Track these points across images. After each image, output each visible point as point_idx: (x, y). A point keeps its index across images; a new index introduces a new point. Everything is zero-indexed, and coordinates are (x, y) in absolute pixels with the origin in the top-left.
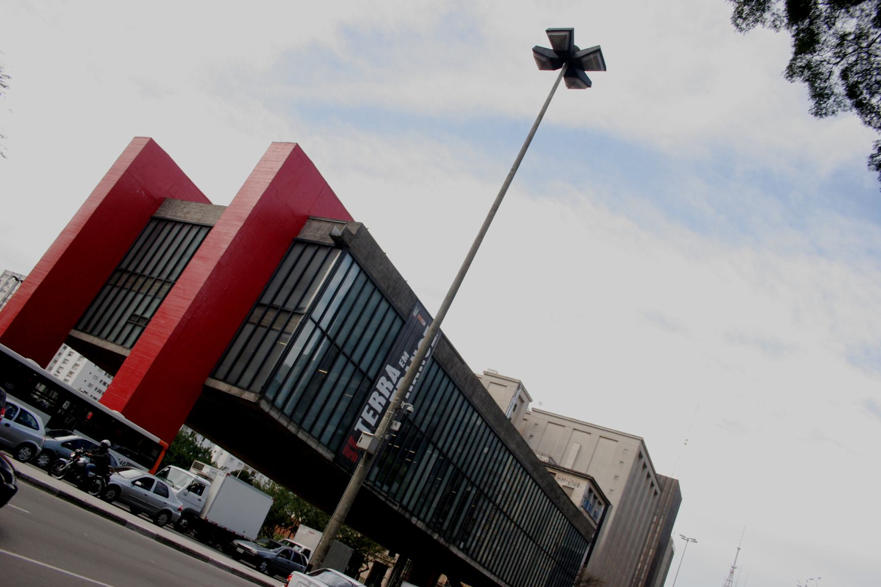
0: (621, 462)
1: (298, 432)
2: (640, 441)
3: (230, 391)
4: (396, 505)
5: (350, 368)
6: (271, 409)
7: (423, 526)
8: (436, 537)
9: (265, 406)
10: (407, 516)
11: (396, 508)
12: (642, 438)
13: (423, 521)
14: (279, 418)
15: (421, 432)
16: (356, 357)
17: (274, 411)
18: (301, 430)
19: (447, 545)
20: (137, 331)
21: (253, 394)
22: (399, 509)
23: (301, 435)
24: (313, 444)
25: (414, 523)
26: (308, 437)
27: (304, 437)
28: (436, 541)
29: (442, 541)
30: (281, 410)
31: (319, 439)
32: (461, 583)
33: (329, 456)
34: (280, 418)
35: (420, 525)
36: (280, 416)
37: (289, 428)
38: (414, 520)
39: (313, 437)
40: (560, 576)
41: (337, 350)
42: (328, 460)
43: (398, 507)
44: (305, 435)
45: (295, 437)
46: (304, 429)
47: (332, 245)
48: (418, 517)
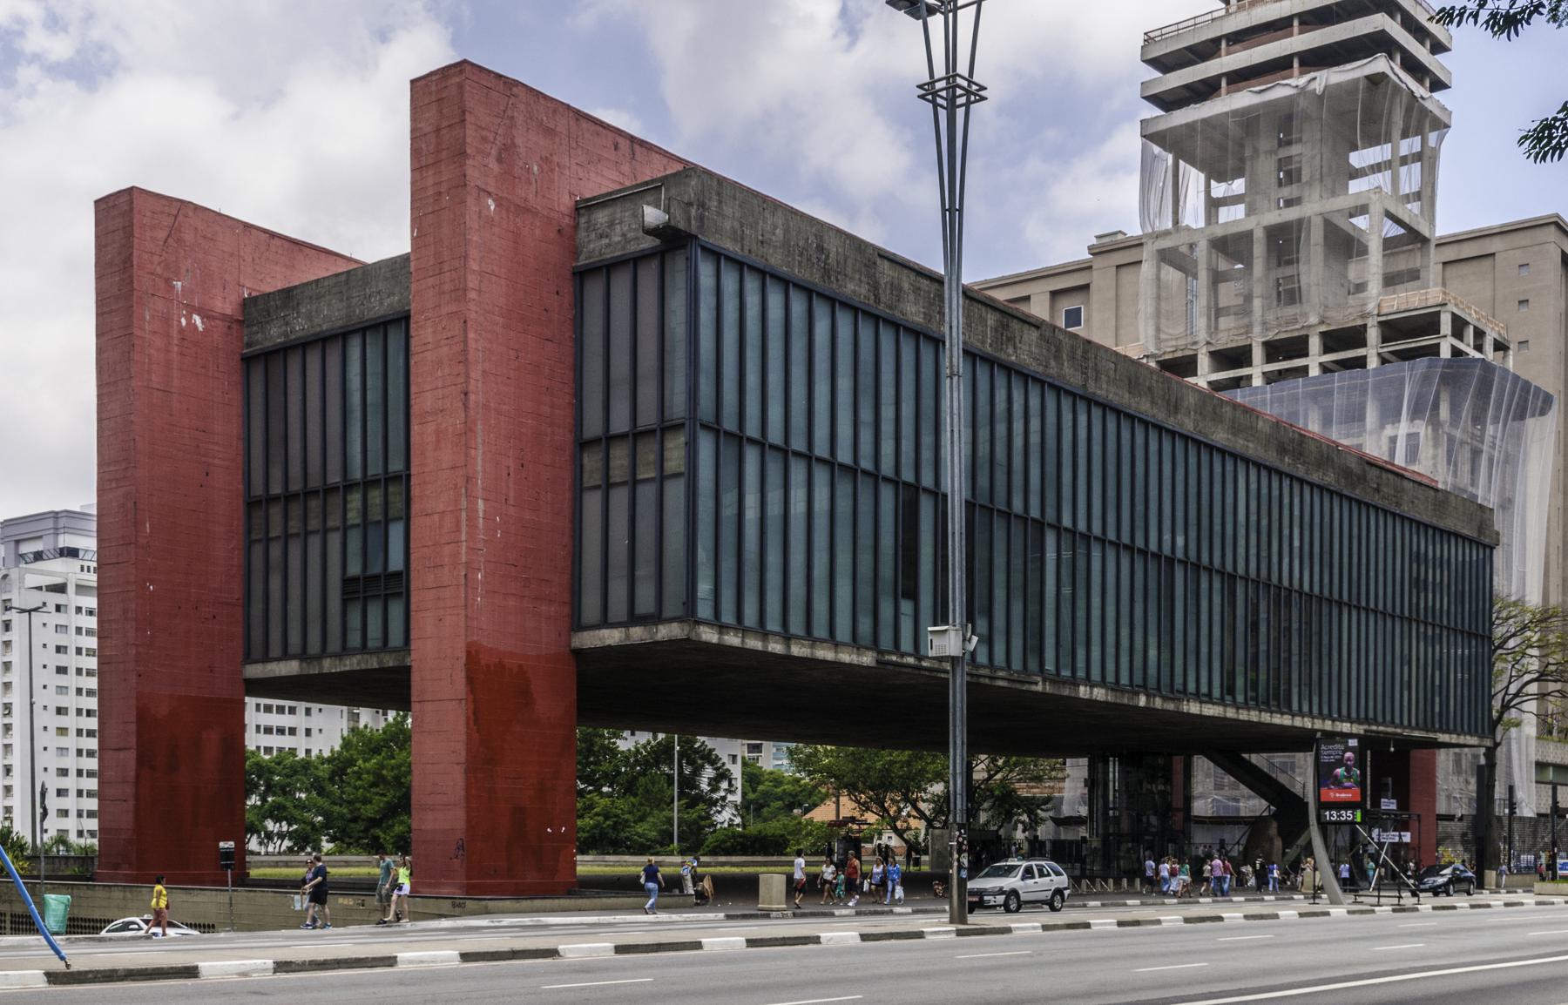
0: (1520, 302)
1: (789, 647)
2: (1553, 228)
3: (628, 636)
4: (1036, 684)
5: (821, 476)
6: (721, 633)
7: (1107, 695)
8: (1142, 701)
9: (709, 635)
10: (1066, 692)
11: (1039, 688)
12: (1557, 216)
13: (1103, 683)
14: (743, 642)
15: (1017, 516)
16: (821, 449)
17: (728, 634)
18: (793, 641)
19: (1171, 706)
20: (396, 609)
21: (675, 625)
22: (1044, 684)
23: (797, 650)
24: (825, 653)
25: (1087, 697)
26: (812, 647)
27: (804, 649)
28: (1146, 709)
29: (1158, 703)
30: (740, 626)
31: (832, 640)
32: (1244, 755)
33: (868, 659)
34: (747, 641)
35: (1099, 694)
36: (743, 637)
37: (770, 649)
38: (1083, 692)
39: (822, 641)
40: (1460, 651)
41: (780, 455)
42: (868, 667)
43: (1040, 683)
44: (803, 645)
45: (788, 658)
46: (797, 637)
47: (659, 249)
48: (1088, 681)
